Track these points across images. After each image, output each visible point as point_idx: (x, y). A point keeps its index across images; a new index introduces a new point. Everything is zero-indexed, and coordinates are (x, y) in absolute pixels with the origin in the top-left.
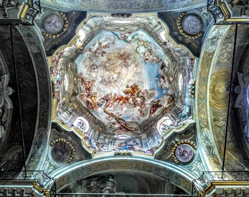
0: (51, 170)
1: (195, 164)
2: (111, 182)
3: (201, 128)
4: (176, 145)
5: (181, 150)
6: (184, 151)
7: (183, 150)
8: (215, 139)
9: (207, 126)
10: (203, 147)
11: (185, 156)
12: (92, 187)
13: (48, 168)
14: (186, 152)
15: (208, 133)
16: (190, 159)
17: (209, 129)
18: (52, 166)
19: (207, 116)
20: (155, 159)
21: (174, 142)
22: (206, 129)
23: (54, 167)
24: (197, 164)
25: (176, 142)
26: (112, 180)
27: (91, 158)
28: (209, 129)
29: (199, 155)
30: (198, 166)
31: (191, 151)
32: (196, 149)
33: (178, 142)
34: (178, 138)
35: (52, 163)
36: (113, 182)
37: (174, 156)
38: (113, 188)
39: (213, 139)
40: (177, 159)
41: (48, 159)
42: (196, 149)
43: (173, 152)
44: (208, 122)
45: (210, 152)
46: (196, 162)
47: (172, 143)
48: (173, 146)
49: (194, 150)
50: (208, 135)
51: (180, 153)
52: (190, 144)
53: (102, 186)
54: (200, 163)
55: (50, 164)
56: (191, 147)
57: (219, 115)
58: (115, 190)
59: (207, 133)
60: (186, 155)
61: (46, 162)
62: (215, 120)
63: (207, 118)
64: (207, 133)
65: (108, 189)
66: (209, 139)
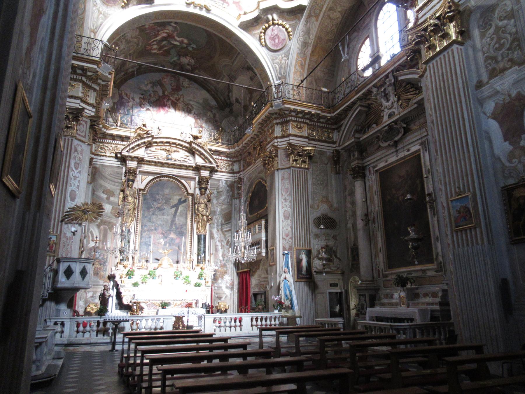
0: (100, 21)
1: (280, 56)
2: (173, 26)
3: (309, 16)
4: (271, 22)
5: (274, 32)
6: (276, 35)
7: (276, 33)
8: (317, 33)
9: (317, 16)
10: (299, 42)
11: (275, 41)
12: (146, 28)
13: (98, 18)
14: (279, 37)
15: (314, 26)
16: (278, 48)
17: (317, 20)
18: (101, 13)
19: (325, 3)
20: (239, 26)
21: (270, 17)
22: (314, 19)
23: (104, 15)
24: (283, 58)
25: (273, 20)
26: (174, 25)
27: (153, 2)
28: (317, 20)
29: (290, 48)
30: (283, 62)
31: (284, 40)
32: (290, 40)
33: (275, 20)
34: (277, 14)
35: (101, 10)
36: (175, 28)
37: (263, 34)
38: (174, 33)
39: (315, 34)
40: (265, 39)
41: (95, 3)
42: (290, 40)
43: (263, 29)
44: (320, 11)
45: (302, 50)
46: (283, 55)
47: (268, 18)
48: (267, 21)
49: (288, 40)
50: (312, 27)
51: (271, 35)
52: (286, 29)
53: (159, 29)
54: (286, 58)
55: (99, 11)
56: (286, 33)
57: (339, 4)
58: (175, 34)
59: (312, 25)
60: (277, 41)
61: (94, 8)
62: (331, 9)
63: (323, 6)
64: (312, 25)
65: (166, 33)
66: (311, 32)
